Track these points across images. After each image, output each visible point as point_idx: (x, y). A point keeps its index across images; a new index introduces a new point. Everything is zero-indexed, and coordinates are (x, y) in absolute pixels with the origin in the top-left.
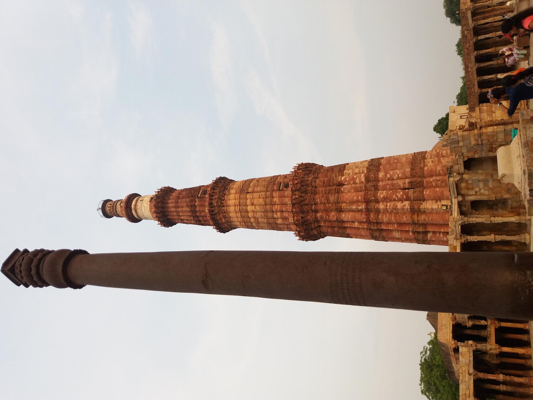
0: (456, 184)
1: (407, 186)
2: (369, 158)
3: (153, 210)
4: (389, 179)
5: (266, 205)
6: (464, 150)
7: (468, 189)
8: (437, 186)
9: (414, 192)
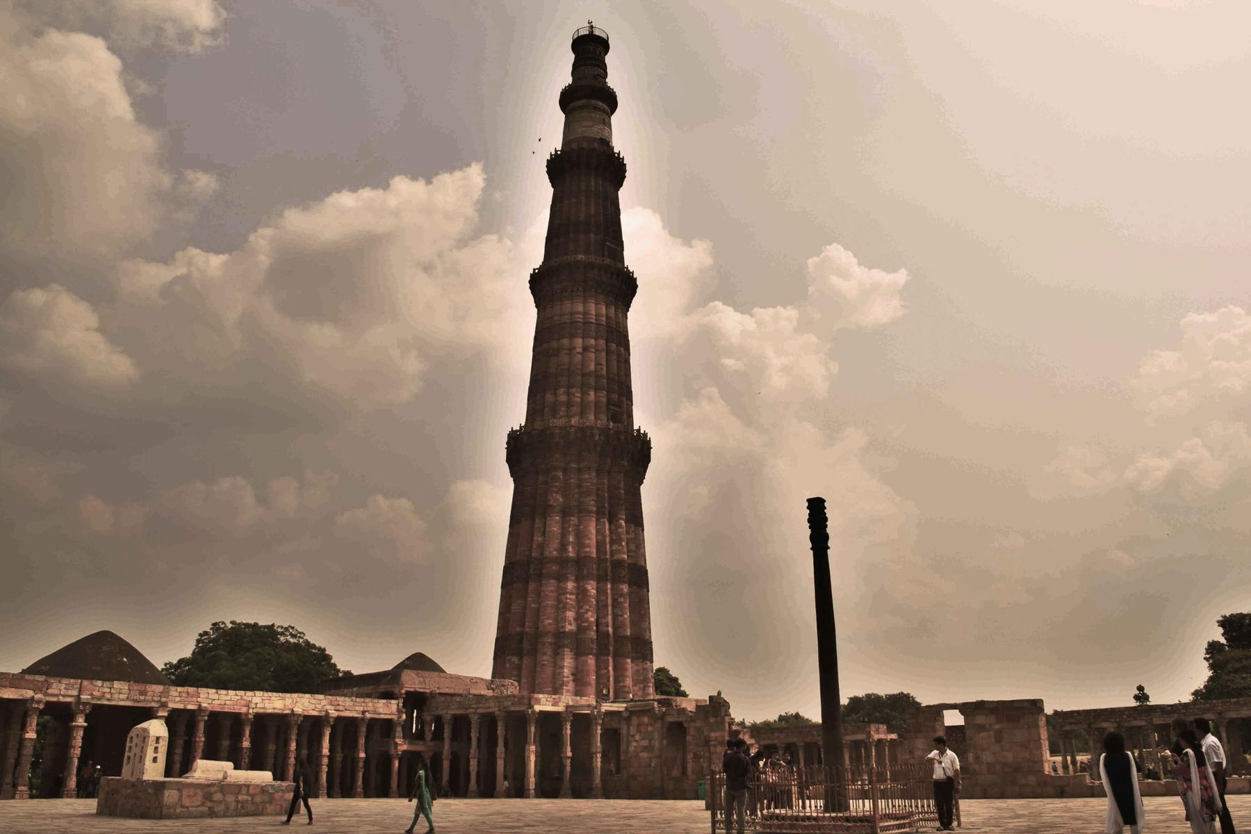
1: (602, 628)
2: (649, 567)
3: (585, 145)
4: (614, 600)
5: (583, 375)
6: (699, 724)
7: (639, 725)
9: (592, 641)
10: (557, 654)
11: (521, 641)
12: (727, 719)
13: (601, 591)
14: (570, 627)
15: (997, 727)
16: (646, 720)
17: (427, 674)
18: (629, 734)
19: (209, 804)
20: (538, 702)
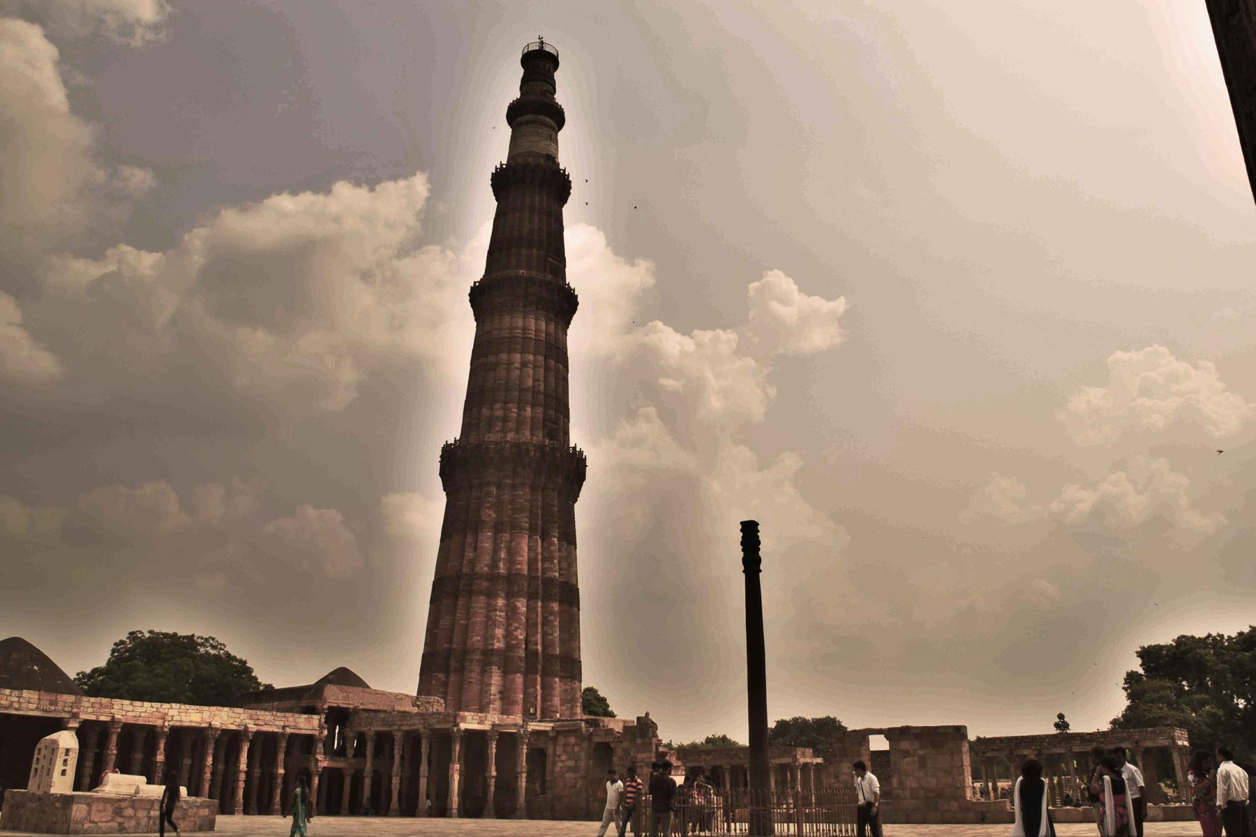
0: (575, 731)
3: (530, 160)
4: (544, 618)
5: (521, 391)
6: (625, 745)
7: (566, 745)
8: (526, 695)
9: (520, 658)
10: (484, 671)
11: (448, 658)
12: (654, 740)
13: (531, 609)
14: (499, 645)
15: (921, 752)
16: (572, 740)
17: (351, 689)
18: (555, 755)
19: (119, 820)
20: (464, 720)
